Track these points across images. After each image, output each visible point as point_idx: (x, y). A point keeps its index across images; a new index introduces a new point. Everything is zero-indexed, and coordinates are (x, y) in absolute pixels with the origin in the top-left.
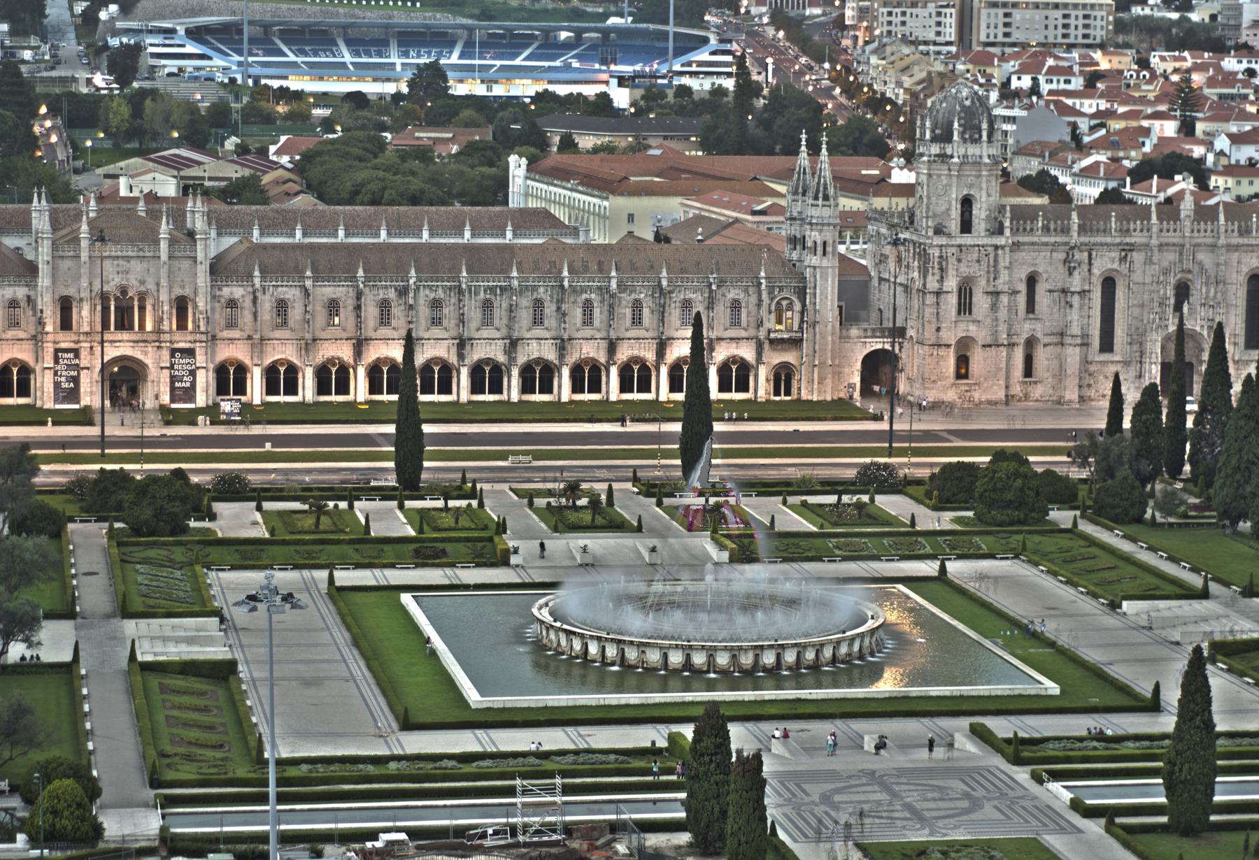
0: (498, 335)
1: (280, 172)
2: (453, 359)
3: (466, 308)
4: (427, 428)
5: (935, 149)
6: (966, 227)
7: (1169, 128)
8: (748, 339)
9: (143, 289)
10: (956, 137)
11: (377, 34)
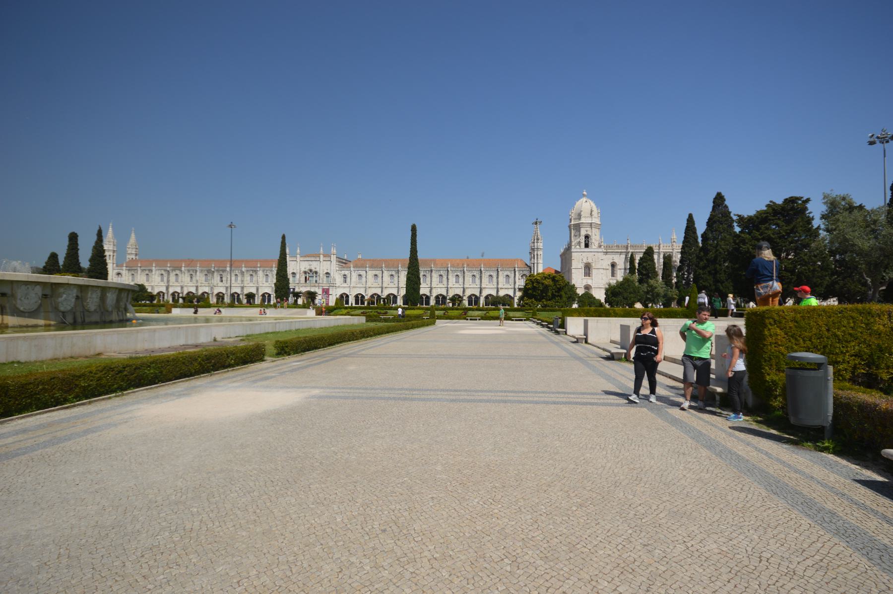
6: (587, 246)
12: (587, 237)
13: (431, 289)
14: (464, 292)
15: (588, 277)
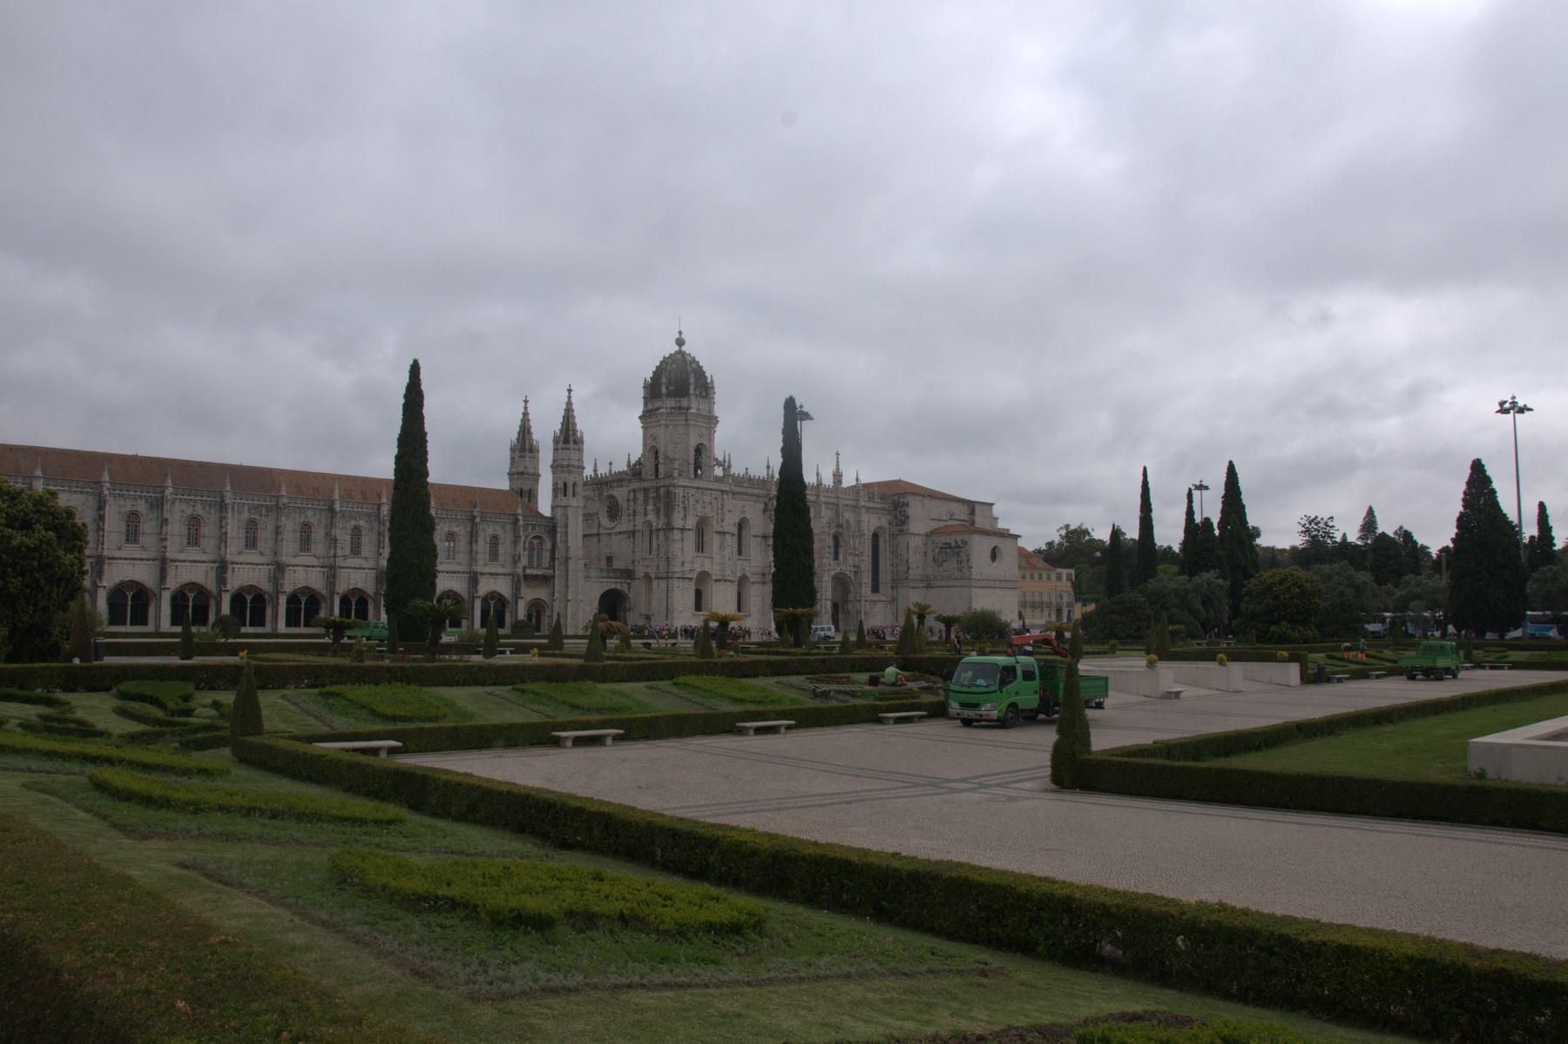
0: (262, 560)
2: (211, 585)
3: (229, 527)
5: (671, 403)
8: (504, 575)
10: (692, 391)
15: (700, 554)
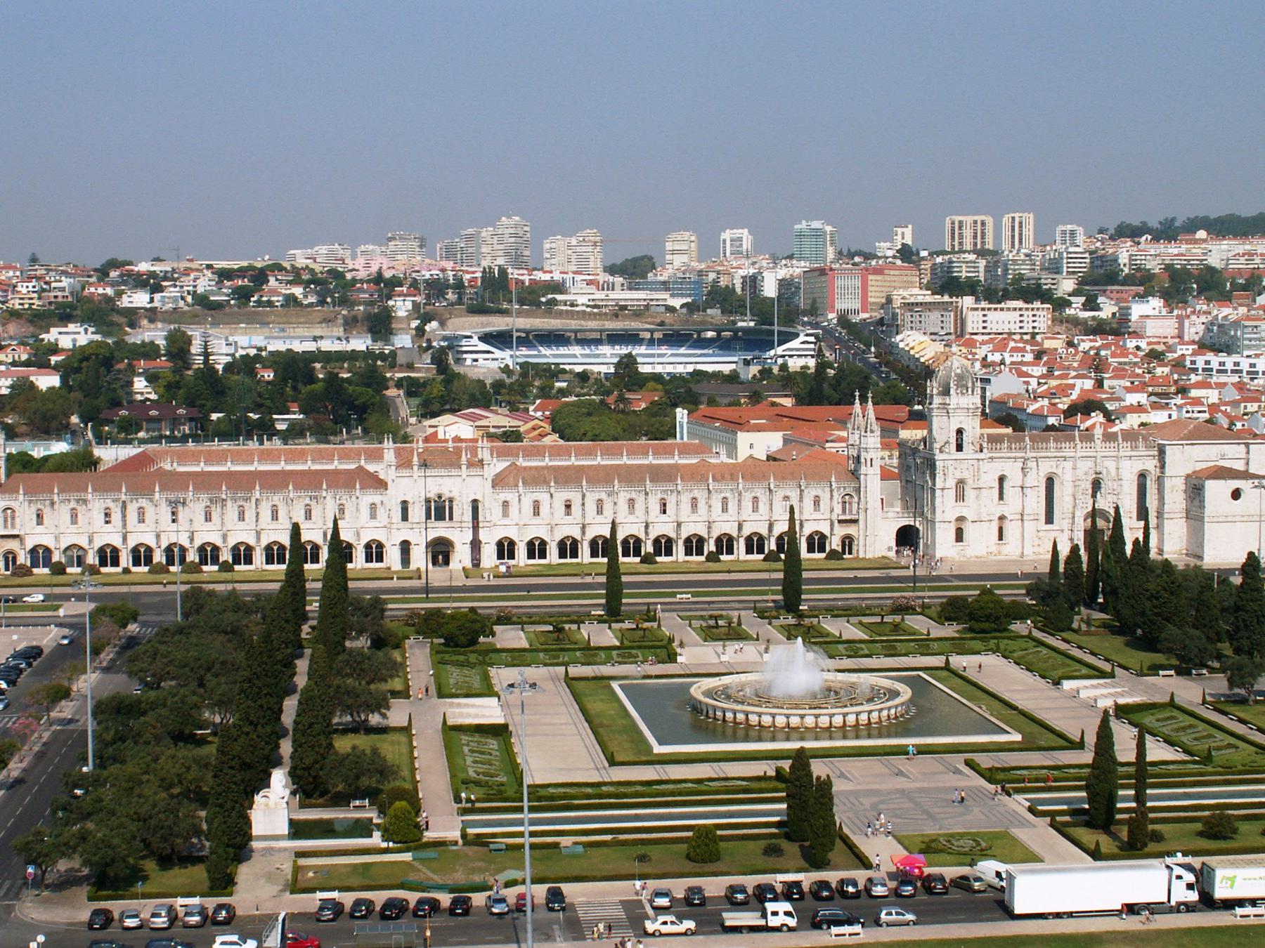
1: (536, 422)
4: (624, 579)
6: (959, 448)
7: (1089, 384)
9: (451, 495)
10: (952, 391)
11: (596, 335)
12: (960, 432)
13: (679, 525)
14: (740, 527)
